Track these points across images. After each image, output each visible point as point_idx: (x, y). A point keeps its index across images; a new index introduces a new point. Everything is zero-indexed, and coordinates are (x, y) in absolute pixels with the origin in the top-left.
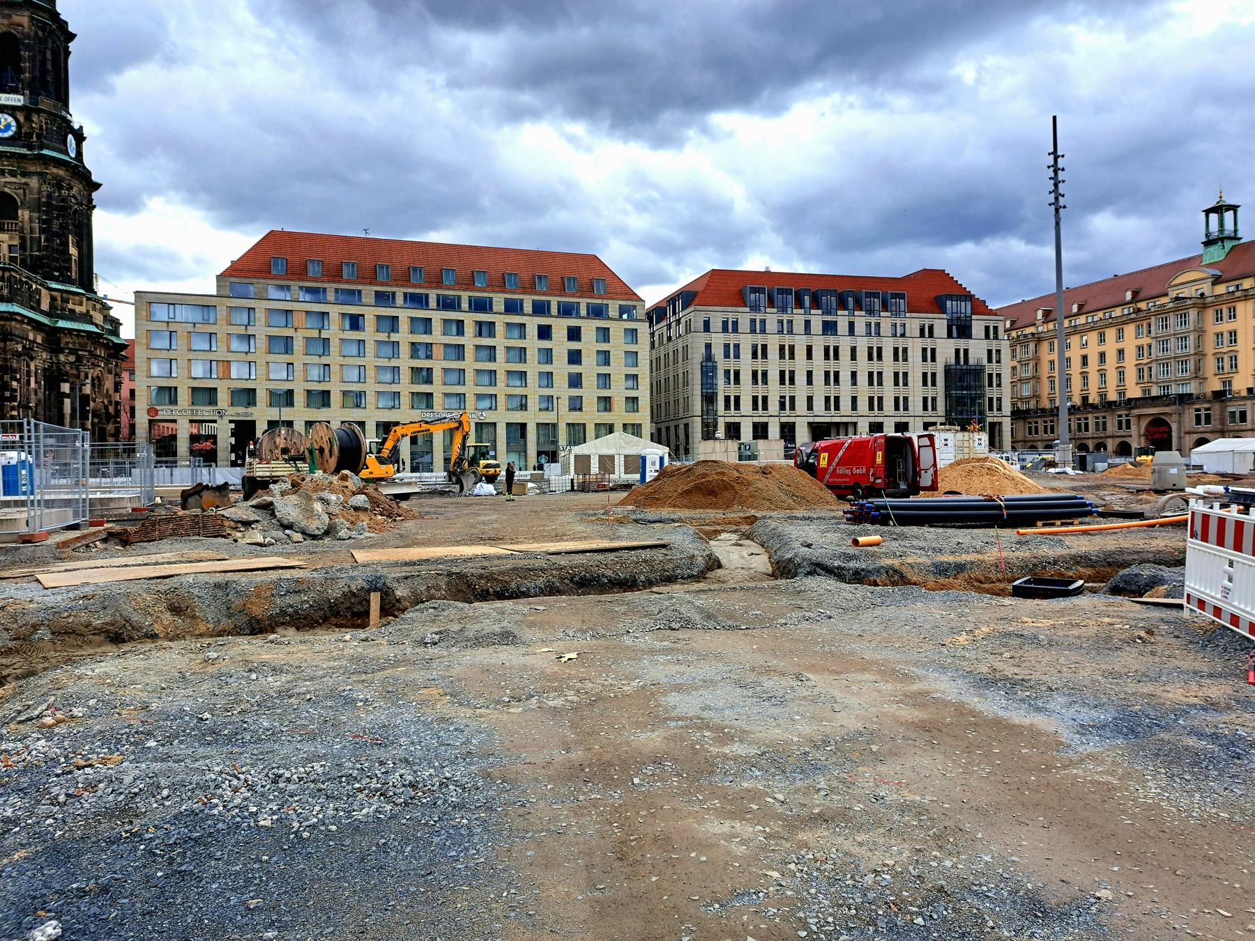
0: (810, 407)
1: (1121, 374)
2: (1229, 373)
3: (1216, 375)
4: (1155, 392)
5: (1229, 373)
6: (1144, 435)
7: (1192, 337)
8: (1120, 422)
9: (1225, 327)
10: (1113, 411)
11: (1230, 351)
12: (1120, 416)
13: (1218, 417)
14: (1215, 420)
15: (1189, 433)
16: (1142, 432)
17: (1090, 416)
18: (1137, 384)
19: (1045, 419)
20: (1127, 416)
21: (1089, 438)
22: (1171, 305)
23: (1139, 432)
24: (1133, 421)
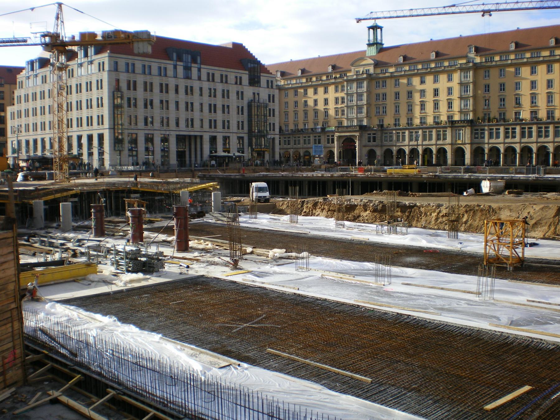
0: (177, 124)
3: (375, 116)
5: (382, 115)
9: (381, 91)
11: (383, 104)
15: (365, 146)
17: (311, 135)
19: (295, 136)
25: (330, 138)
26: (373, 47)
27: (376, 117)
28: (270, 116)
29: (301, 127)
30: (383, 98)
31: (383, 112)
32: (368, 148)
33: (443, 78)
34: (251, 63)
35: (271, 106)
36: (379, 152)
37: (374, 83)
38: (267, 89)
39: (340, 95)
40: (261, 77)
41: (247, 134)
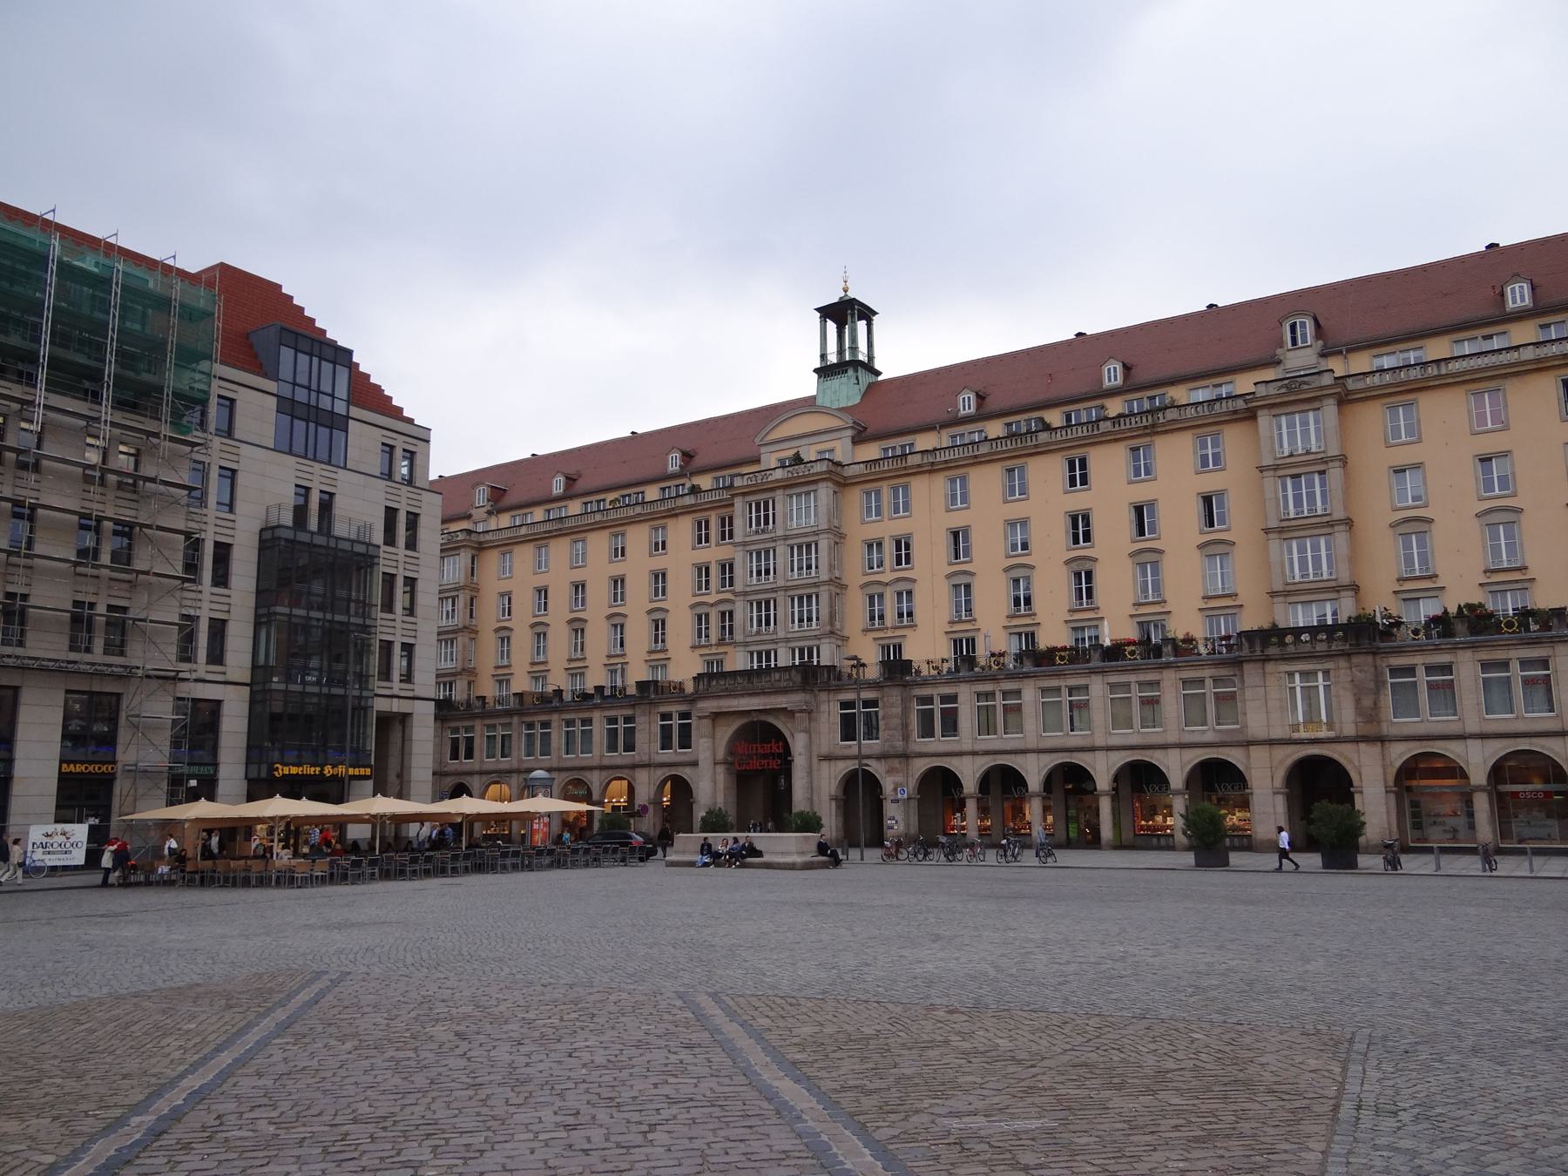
1: (659, 626)
3: (866, 631)
4: (738, 661)
6: (725, 762)
8: (666, 732)
10: (652, 704)
11: (899, 580)
13: (896, 721)
14: (888, 728)
15: (828, 758)
16: (721, 754)
18: (694, 647)
21: (591, 769)
22: (779, 474)
24: (699, 729)
25: (676, 722)
26: (844, 380)
28: (388, 606)
29: (558, 679)
30: (899, 557)
31: (901, 615)
32: (844, 767)
34: (297, 350)
35: (394, 560)
36: (898, 785)
37: (855, 496)
39: (714, 554)
41: (248, 688)
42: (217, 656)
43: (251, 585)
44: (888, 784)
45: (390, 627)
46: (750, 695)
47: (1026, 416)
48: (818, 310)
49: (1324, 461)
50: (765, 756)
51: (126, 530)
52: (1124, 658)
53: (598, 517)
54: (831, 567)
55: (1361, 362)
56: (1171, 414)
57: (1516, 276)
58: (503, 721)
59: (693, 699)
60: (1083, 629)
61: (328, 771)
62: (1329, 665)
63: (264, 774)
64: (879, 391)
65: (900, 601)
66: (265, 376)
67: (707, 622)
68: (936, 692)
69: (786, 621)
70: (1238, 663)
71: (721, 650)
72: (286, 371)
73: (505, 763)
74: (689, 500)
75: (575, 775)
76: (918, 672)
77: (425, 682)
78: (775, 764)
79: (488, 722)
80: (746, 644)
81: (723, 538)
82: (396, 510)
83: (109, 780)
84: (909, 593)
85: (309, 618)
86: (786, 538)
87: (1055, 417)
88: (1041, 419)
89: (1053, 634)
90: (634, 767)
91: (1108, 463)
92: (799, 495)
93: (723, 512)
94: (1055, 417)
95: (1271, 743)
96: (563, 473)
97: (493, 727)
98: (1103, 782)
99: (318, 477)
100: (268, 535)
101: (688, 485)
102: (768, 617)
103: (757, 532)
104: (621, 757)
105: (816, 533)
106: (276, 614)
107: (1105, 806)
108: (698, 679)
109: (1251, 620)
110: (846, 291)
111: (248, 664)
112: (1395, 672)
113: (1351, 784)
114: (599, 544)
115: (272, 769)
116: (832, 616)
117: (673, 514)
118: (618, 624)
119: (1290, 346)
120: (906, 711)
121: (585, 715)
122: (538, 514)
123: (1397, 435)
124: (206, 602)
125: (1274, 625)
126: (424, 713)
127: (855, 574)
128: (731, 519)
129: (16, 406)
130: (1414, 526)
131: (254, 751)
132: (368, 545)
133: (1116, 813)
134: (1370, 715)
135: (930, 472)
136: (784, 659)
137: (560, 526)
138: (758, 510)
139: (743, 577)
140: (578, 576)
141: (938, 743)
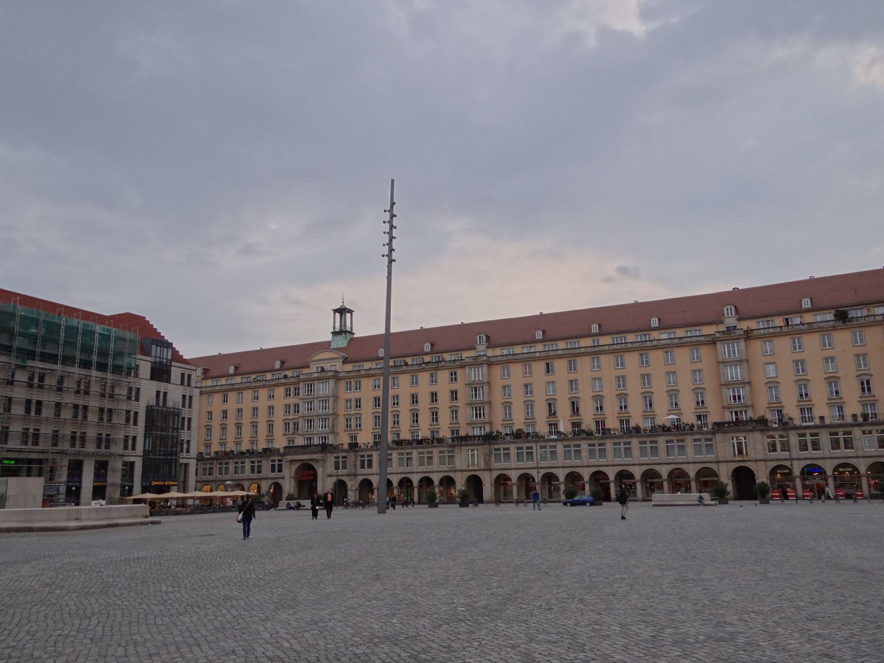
1: (271, 426)
2: (355, 430)
3: (345, 431)
4: (300, 441)
5: (355, 430)
7: (331, 400)
8: (273, 466)
10: (268, 456)
12: (273, 461)
13: (352, 463)
14: (350, 466)
15: (330, 476)
16: (293, 474)
18: (284, 435)
19: (220, 461)
20: (279, 461)
21: (244, 480)
22: (316, 375)
23: (290, 475)
24: (285, 466)
26: (341, 337)
27: (347, 433)
28: (183, 428)
29: (230, 447)
31: (357, 426)
32: (334, 479)
33: (443, 376)
34: (157, 346)
35: (185, 413)
36: (352, 485)
37: (343, 384)
38: (182, 387)
39: (292, 401)
40: (172, 368)
42: (134, 448)
43: (144, 424)
44: (349, 485)
45: (184, 435)
46: (304, 454)
47: (401, 359)
48: (333, 310)
49: (483, 383)
50: (308, 475)
51: (110, 411)
52: (423, 444)
53: (248, 384)
54: (333, 409)
55: (498, 352)
56: (443, 364)
57: (538, 329)
58: (210, 462)
59: (283, 455)
60: (414, 432)
61: (166, 483)
62: (478, 447)
63: (148, 484)
64: (355, 342)
65: (357, 421)
66: (147, 355)
67: (289, 426)
68: (366, 454)
69: (318, 428)
70: (453, 446)
71: (293, 436)
72: (153, 354)
73: (210, 478)
74: (283, 381)
75: (238, 482)
76: (360, 447)
77: (194, 452)
78: (312, 478)
79: (204, 462)
80: (303, 435)
81: (295, 395)
82: (186, 395)
83: (105, 487)
84: (360, 418)
85: (161, 435)
86: (318, 398)
87: (409, 360)
88: (405, 361)
89: (406, 435)
90: (261, 479)
91: (424, 378)
92: (323, 383)
93: (296, 386)
94: (409, 360)
95: (462, 471)
96: (234, 365)
97: (205, 464)
98: (415, 483)
99: (162, 386)
100: (149, 408)
101: (283, 374)
102: (311, 425)
103: (308, 395)
104: (256, 475)
105: (328, 397)
106: (152, 434)
107: (416, 491)
108: (285, 448)
109: (462, 433)
110: (343, 302)
111: (142, 449)
112: (496, 450)
113: (482, 483)
114: (248, 395)
115: (150, 483)
116: (333, 426)
117: (277, 385)
118: (255, 425)
119: (479, 344)
120: (356, 460)
121: (242, 460)
122: (223, 381)
123: (504, 376)
124: (131, 431)
125: (467, 434)
126: (193, 464)
127: (342, 411)
128: (298, 388)
129: (84, 376)
130: (508, 405)
131: (144, 476)
132: (178, 409)
133: (419, 492)
134: (488, 462)
135: (368, 377)
136: (316, 441)
137: (233, 387)
138: (308, 387)
139: (303, 410)
140: (239, 406)
141: (366, 470)
